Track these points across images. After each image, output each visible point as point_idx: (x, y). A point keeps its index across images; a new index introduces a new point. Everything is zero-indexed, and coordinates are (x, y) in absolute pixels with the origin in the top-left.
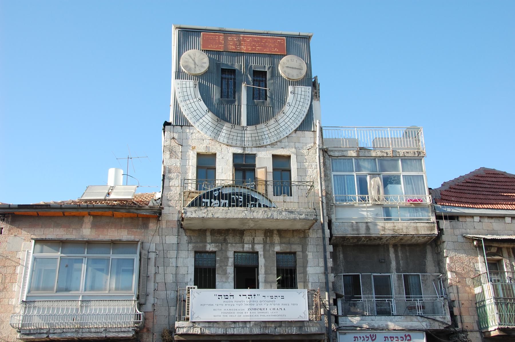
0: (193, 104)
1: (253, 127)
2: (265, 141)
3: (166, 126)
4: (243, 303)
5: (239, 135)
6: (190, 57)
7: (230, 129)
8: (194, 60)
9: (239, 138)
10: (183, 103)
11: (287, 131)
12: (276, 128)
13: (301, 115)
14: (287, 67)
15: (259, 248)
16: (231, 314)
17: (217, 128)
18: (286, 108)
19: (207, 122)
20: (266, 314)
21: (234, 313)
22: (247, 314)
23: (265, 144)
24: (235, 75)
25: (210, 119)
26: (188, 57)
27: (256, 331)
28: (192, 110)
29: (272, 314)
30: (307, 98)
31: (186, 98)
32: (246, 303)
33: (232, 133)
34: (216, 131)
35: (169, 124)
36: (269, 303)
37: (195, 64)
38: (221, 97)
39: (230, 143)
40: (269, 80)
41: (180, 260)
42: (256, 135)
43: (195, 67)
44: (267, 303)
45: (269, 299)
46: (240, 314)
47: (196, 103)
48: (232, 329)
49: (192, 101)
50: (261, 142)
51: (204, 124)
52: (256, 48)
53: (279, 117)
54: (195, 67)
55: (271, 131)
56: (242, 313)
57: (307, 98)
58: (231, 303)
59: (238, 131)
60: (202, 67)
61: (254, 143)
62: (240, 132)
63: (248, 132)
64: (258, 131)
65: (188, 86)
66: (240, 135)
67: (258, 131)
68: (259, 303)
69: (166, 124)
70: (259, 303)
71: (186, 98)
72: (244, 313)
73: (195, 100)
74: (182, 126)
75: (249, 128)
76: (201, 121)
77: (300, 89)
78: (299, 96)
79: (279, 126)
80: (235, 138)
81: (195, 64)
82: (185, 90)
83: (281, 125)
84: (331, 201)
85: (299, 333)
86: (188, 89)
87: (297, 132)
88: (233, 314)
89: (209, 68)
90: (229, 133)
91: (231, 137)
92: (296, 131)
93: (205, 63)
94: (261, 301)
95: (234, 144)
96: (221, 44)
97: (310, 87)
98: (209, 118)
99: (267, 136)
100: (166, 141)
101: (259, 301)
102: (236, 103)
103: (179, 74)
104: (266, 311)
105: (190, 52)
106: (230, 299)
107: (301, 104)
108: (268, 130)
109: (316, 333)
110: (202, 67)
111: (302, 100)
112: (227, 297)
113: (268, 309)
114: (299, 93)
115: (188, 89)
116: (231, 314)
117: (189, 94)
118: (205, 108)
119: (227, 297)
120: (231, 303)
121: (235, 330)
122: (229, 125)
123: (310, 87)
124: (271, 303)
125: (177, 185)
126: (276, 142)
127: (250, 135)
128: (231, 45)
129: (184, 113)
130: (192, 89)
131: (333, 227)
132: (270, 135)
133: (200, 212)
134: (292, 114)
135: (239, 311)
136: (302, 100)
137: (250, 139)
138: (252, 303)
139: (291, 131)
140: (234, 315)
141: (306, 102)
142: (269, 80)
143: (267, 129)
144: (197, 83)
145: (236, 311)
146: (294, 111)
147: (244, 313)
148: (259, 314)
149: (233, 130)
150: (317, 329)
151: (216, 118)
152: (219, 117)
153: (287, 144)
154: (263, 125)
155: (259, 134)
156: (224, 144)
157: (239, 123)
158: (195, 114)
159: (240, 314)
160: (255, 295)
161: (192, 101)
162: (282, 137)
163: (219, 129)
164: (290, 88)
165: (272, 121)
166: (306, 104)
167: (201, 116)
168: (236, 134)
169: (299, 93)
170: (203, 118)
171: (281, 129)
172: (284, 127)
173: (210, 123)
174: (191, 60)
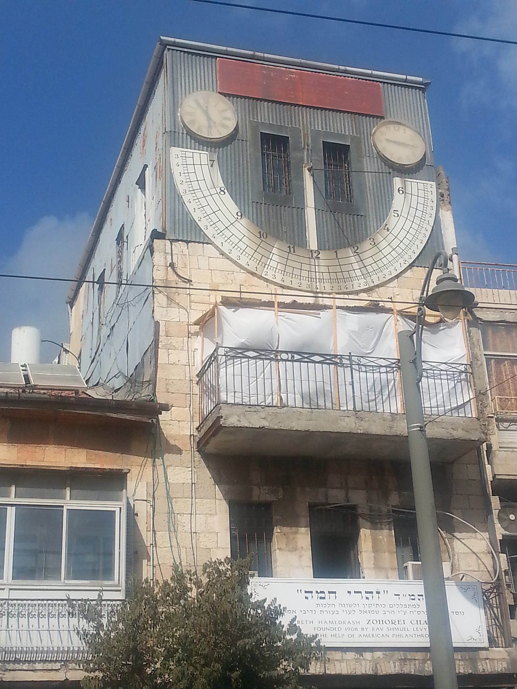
2: (356, 283)
3: (155, 240)
4: (357, 609)
5: (304, 267)
8: (206, 112)
9: (305, 274)
11: (397, 265)
12: (376, 258)
13: (421, 237)
14: (388, 140)
15: (358, 498)
16: (334, 632)
17: (260, 250)
18: (392, 220)
19: (240, 236)
20: (404, 633)
21: (340, 629)
22: (365, 632)
23: (357, 288)
24: (286, 148)
27: (390, 668)
29: (416, 632)
30: (430, 204)
31: (195, 185)
32: (362, 608)
36: (408, 610)
37: (209, 119)
39: (287, 283)
41: (201, 519)
42: (338, 269)
43: (210, 127)
44: (404, 609)
45: (406, 600)
46: (351, 632)
47: (216, 197)
48: (337, 664)
49: (206, 193)
50: (349, 284)
55: (366, 262)
56: (356, 629)
57: (430, 204)
58: (331, 609)
59: (302, 260)
60: (224, 126)
61: (336, 285)
62: (307, 261)
64: (342, 262)
67: (342, 262)
68: (387, 608)
70: (387, 608)
71: (195, 185)
72: (359, 629)
73: (213, 191)
74: (187, 242)
76: (228, 234)
77: (414, 185)
78: (415, 198)
80: (297, 272)
81: (209, 119)
82: (191, 169)
83: (385, 252)
84: (488, 408)
85: (470, 671)
86: (198, 167)
87: (415, 268)
88: (337, 632)
89: (236, 129)
91: (289, 270)
92: (411, 266)
93: (229, 119)
94: (391, 606)
95: (295, 285)
97: (434, 183)
101: (387, 606)
104: (402, 626)
105: (200, 96)
106: (330, 599)
107: (419, 214)
109: (504, 671)
110: (224, 126)
111: (420, 207)
112: (322, 595)
113: (407, 622)
114: (415, 192)
115: (198, 167)
116: (334, 632)
118: (235, 209)
119: (322, 595)
120: (331, 609)
121: (344, 665)
123: (434, 183)
124: (412, 609)
125: (185, 362)
126: (378, 286)
127: (324, 269)
129: (196, 216)
130: (206, 168)
131: (496, 461)
133: (255, 416)
135: (350, 626)
136: (420, 207)
137: (326, 276)
138: (373, 608)
139: (404, 266)
140: (340, 633)
141: (429, 211)
144: (215, 158)
145: (343, 626)
147: (359, 629)
148: (390, 633)
150: (505, 665)
151: (256, 231)
152: (261, 228)
153: (397, 291)
154: (350, 252)
155: (344, 268)
156: (275, 284)
157: (303, 243)
159: (351, 632)
160: (378, 593)
161: (206, 193)
162: (388, 277)
163: (266, 254)
165: (367, 245)
168: (298, 266)
170: (231, 228)
173: (245, 240)
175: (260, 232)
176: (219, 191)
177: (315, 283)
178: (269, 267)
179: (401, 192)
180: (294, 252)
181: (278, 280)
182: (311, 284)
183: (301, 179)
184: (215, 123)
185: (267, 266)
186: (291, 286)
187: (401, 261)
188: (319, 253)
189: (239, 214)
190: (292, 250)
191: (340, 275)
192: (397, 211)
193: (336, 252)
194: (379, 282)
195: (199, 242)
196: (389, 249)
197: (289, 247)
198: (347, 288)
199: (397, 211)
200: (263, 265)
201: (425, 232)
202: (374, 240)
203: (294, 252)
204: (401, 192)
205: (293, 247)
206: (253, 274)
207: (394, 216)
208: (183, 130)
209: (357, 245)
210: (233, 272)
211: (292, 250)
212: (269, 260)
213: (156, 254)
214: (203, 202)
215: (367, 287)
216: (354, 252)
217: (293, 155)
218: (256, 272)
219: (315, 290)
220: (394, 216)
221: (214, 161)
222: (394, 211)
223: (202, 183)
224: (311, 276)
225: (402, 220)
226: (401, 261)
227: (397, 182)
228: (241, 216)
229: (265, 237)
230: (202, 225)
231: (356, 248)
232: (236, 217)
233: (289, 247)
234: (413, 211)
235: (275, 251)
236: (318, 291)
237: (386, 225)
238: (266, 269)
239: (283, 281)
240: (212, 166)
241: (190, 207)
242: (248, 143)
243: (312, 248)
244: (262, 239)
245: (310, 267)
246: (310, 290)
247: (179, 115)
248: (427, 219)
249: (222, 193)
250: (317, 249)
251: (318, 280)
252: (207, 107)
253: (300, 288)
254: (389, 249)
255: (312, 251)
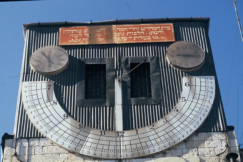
0: (45, 110)
1: (133, 132)
3: (6, 140)
5: (111, 143)
6: (44, 54)
7: (98, 137)
9: (111, 148)
10: (32, 110)
12: (167, 130)
17: (79, 136)
23: (152, 152)
25: (69, 126)
26: (42, 56)
28: (44, 116)
31: (36, 102)
33: (100, 142)
34: (77, 141)
35: (12, 137)
38: (86, 98)
39: (98, 155)
40: (154, 72)
43: (50, 66)
47: (50, 108)
49: (43, 106)
51: (61, 132)
52: (133, 38)
53: (170, 116)
54: (50, 66)
55: (160, 134)
59: (110, 139)
62: (114, 139)
63: (125, 139)
65: (39, 87)
66: (114, 143)
67: (140, 136)
69: (6, 137)
75: (126, 133)
76: (56, 129)
79: (172, 128)
80: (106, 147)
83: (175, 125)
87: (200, 134)
90: (97, 141)
91: (100, 147)
93: (64, 60)
96: (87, 37)
98: (68, 123)
99: (154, 142)
100: (5, 159)
102: (107, 104)
103: (28, 75)
108: (156, 136)
110: (60, 64)
117: (40, 96)
118: (62, 112)
122: (98, 132)
128: (100, 37)
132: (158, 140)
134: (189, 111)
137: (128, 147)
142: (152, 73)
143: (153, 132)
146: (192, 107)
149: (102, 138)
151: (77, 124)
153: (185, 150)
154: (147, 129)
157: (112, 128)
158: (47, 121)
163: (84, 138)
164: (185, 80)
166: (208, 98)
167: (56, 122)
168: (108, 143)
169: (198, 84)
170: (60, 126)
171: (175, 131)
172: (179, 129)
173: (69, 132)
174: (44, 58)
175: (80, 125)
176: (52, 103)
177: (119, 153)
178: (85, 147)
179: (187, 85)
180: (105, 134)
181: (91, 154)
182: (117, 154)
183: (113, 87)
184: (53, 63)
185: (83, 146)
186: (101, 157)
187: (188, 130)
188: (124, 133)
189: (66, 115)
190: (103, 133)
191: (139, 146)
192: (185, 98)
193: (137, 130)
194: (170, 146)
195: (37, 137)
196: (178, 123)
197: (101, 132)
198: (144, 154)
199: (185, 98)
200: (81, 146)
201: (207, 108)
202: (166, 118)
203: (105, 134)
204: (187, 85)
205: (104, 132)
206: (73, 153)
207: (182, 101)
208: (32, 71)
209: (154, 124)
210: (60, 153)
211: (103, 133)
212: (86, 142)
213: (6, 148)
214: (41, 111)
215: (160, 150)
216: (151, 129)
217: (109, 75)
218: (76, 151)
219: (119, 158)
220: (182, 101)
221: (51, 86)
222: (182, 98)
223: (41, 101)
224: (116, 148)
225: (189, 103)
226: (188, 130)
227: (185, 80)
228: (67, 117)
229: (83, 127)
230: (38, 127)
231: (152, 126)
232: (63, 117)
233: (101, 132)
234: (197, 96)
235: (90, 135)
236: (121, 158)
237: (176, 108)
238: (82, 148)
239: (95, 155)
240: (49, 89)
241: (30, 117)
242: (76, 72)
243: (118, 130)
244: (81, 129)
245: (116, 143)
246: (115, 158)
247: (30, 63)
248: (208, 100)
249: (55, 104)
250: (122, 130)
251: (122, 151)
252: (49, 56)
253: (107, 158)
254: (178, 123)
255: (118, 132)
